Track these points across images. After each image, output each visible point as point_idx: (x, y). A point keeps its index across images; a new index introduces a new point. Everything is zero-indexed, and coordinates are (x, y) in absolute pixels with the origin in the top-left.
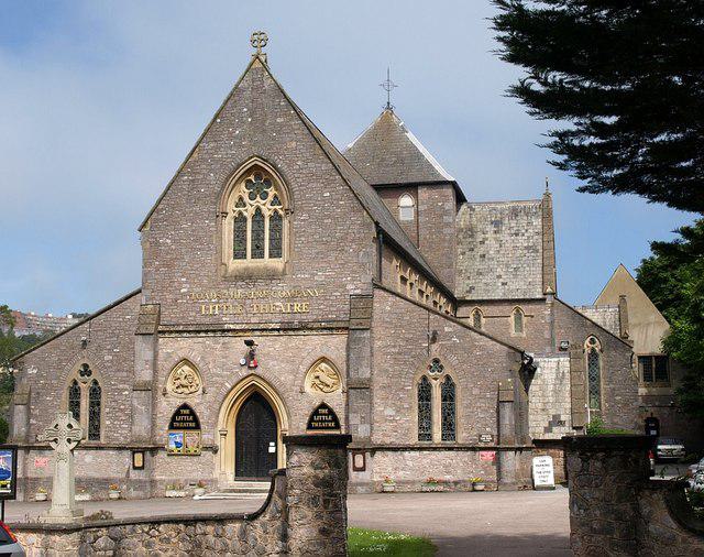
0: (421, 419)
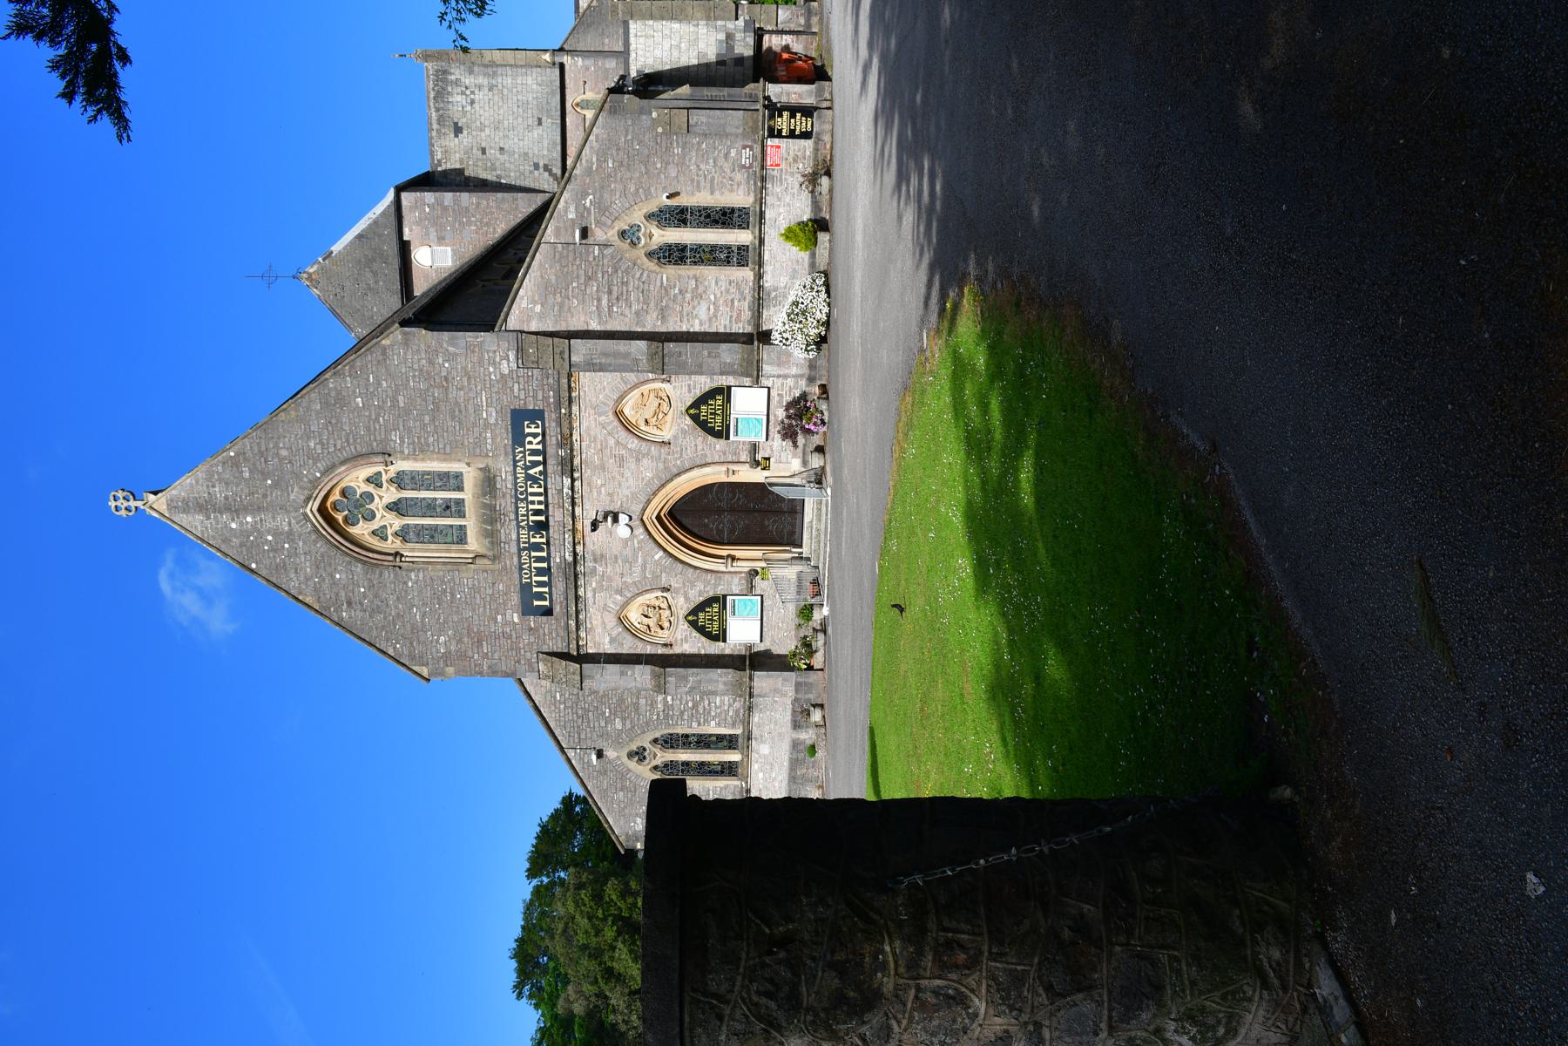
0: (714, 261)
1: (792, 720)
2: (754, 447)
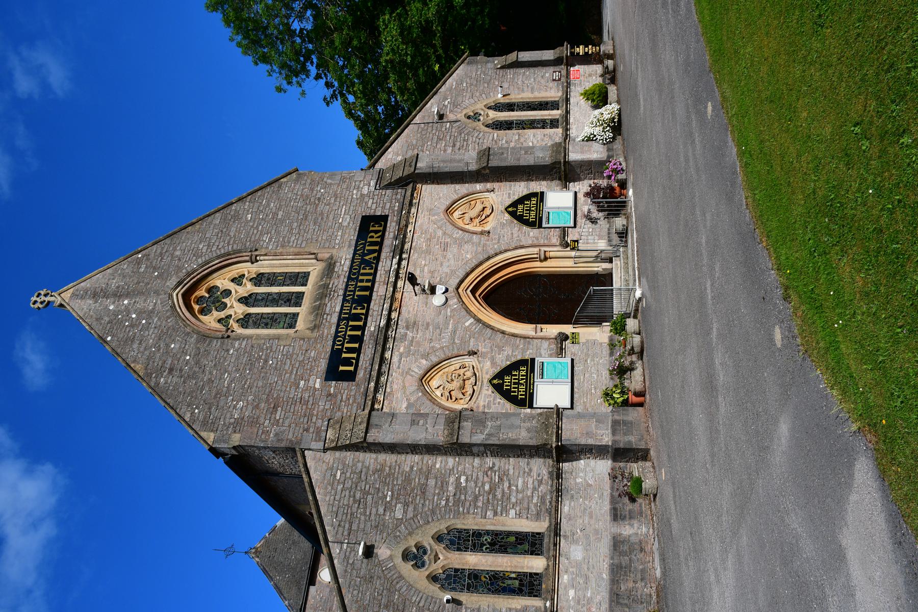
1: (611, 509)
2: (564, 231)
